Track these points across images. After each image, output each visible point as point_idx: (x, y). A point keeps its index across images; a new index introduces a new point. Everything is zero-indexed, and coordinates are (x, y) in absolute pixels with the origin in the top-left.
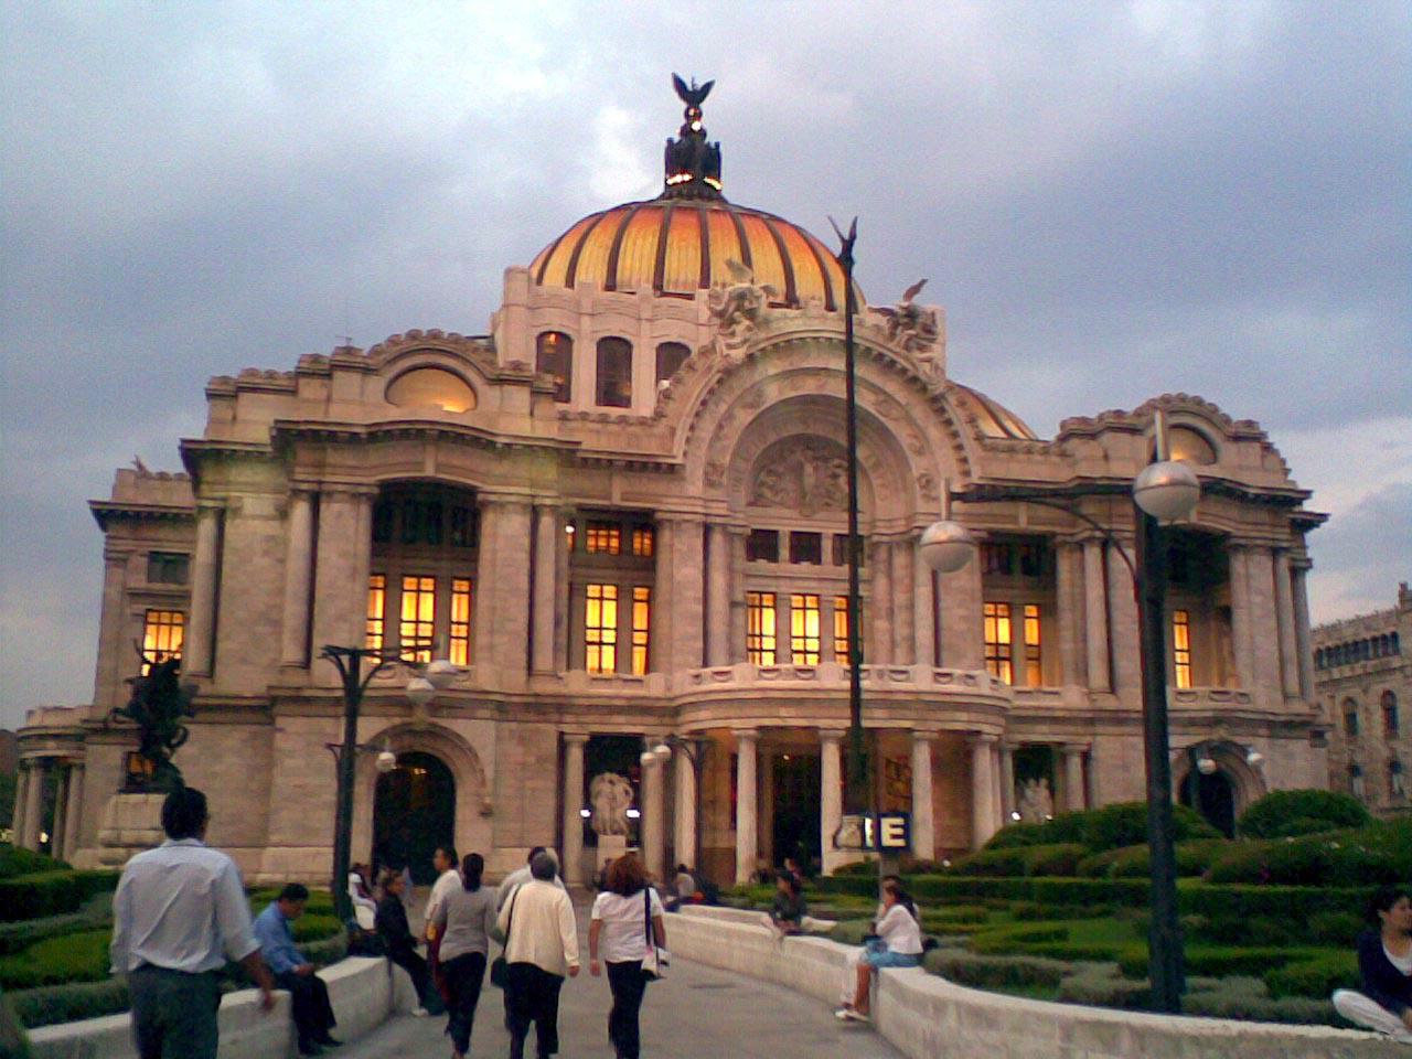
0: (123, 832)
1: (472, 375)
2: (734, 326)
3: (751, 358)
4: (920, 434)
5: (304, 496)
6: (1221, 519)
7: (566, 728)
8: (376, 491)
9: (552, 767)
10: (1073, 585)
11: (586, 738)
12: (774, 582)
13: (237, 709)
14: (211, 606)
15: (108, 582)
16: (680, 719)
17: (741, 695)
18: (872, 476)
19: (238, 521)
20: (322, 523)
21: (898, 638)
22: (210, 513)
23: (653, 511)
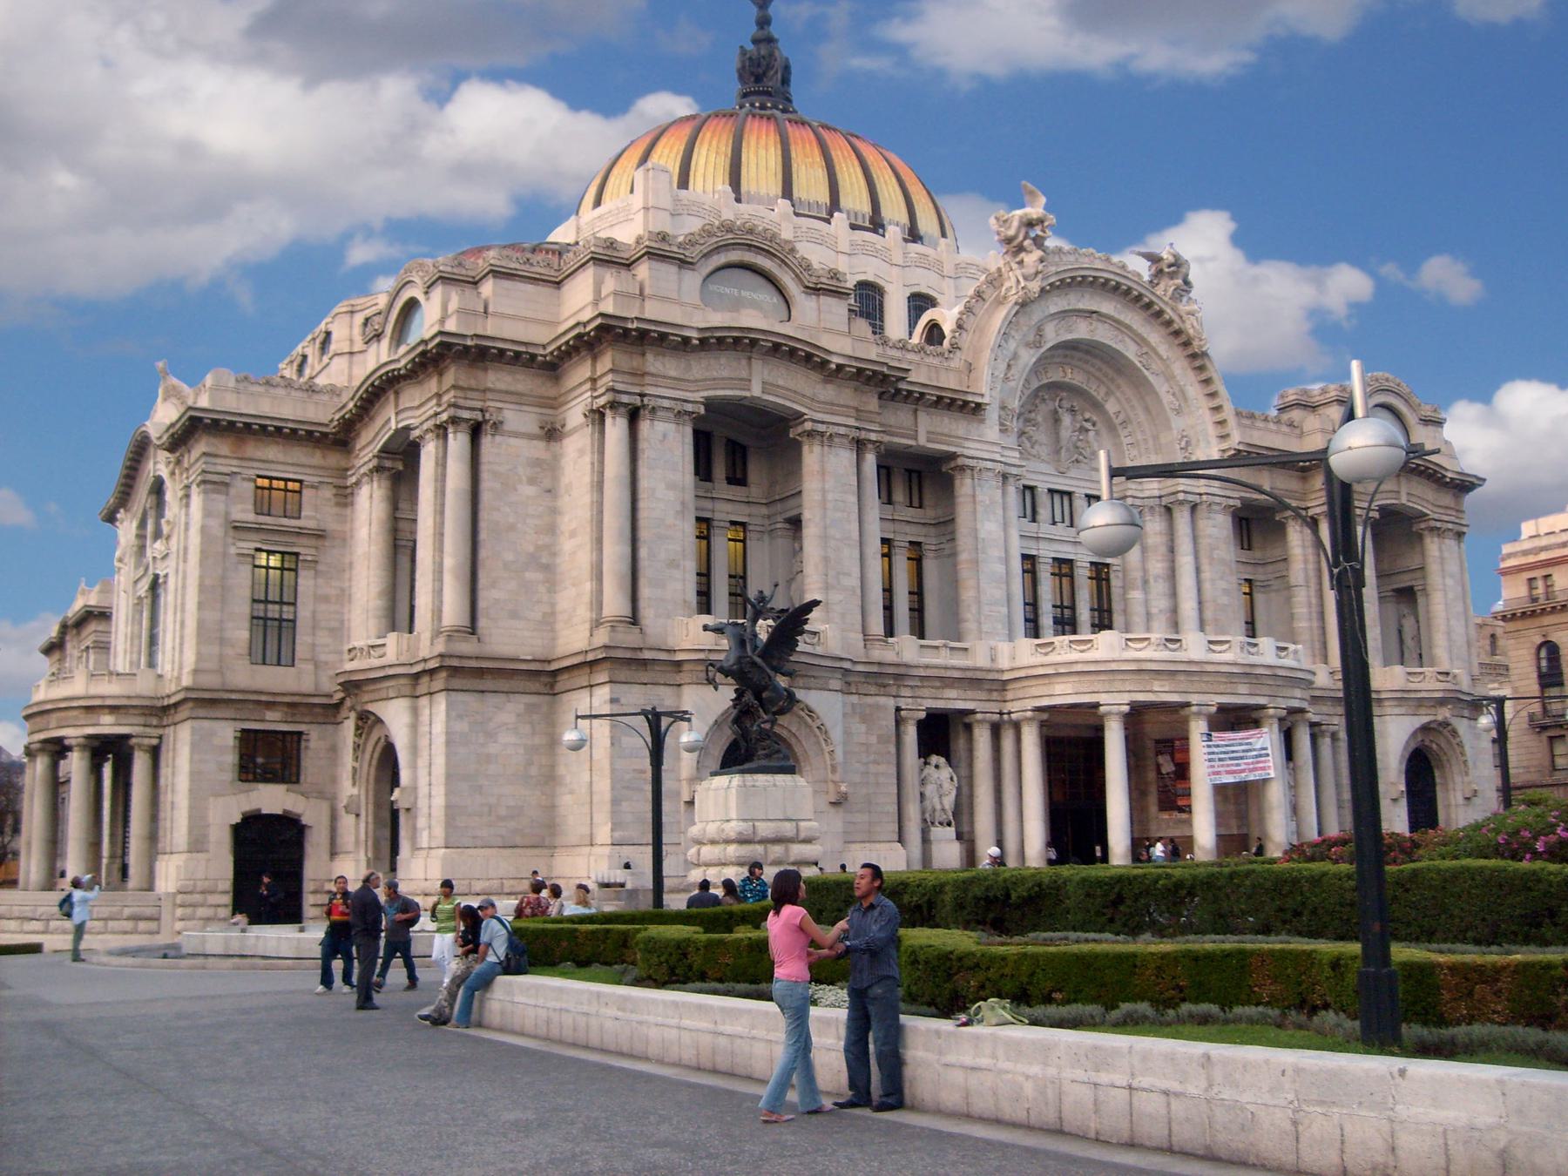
0: (802, 824)
1: (787, 280)
2: (1023, 255)
3: (1043, 290)
4: (1181, 394)
5: (622, 410)
6: (1413, 496)
7: (902, 703)
8: (702, 411)
9: (893, 749)
10: (1306, 562)
11: (923, 715)
12: (1032, 544)
13: (514, 673)
14: (469, 543)
15: (207, 513)
16: (1010, 695)
17: (1114, 666)
18: (1123, 433)
19: (498, 438)
20: (642, 445)
21: (1154, 611)
22: (464, 426)
23: (953, 456)
